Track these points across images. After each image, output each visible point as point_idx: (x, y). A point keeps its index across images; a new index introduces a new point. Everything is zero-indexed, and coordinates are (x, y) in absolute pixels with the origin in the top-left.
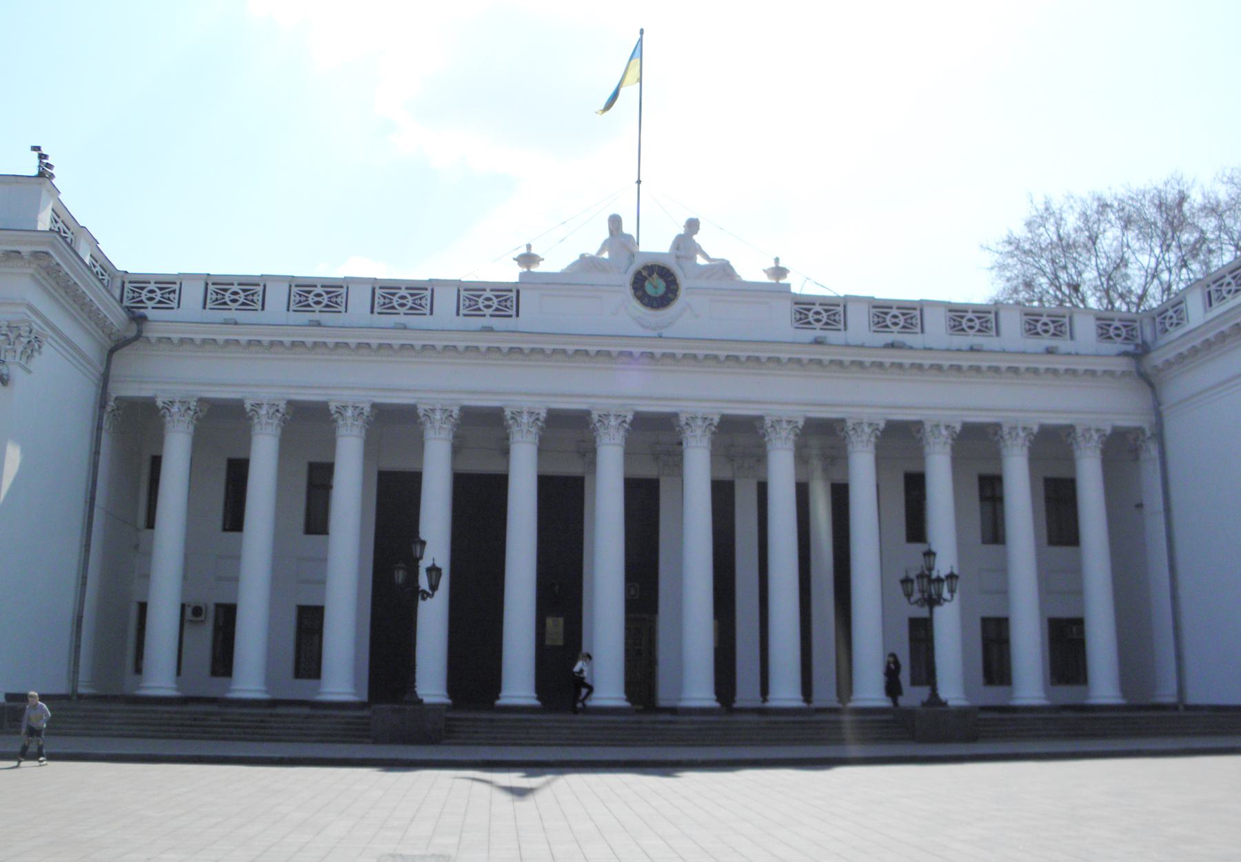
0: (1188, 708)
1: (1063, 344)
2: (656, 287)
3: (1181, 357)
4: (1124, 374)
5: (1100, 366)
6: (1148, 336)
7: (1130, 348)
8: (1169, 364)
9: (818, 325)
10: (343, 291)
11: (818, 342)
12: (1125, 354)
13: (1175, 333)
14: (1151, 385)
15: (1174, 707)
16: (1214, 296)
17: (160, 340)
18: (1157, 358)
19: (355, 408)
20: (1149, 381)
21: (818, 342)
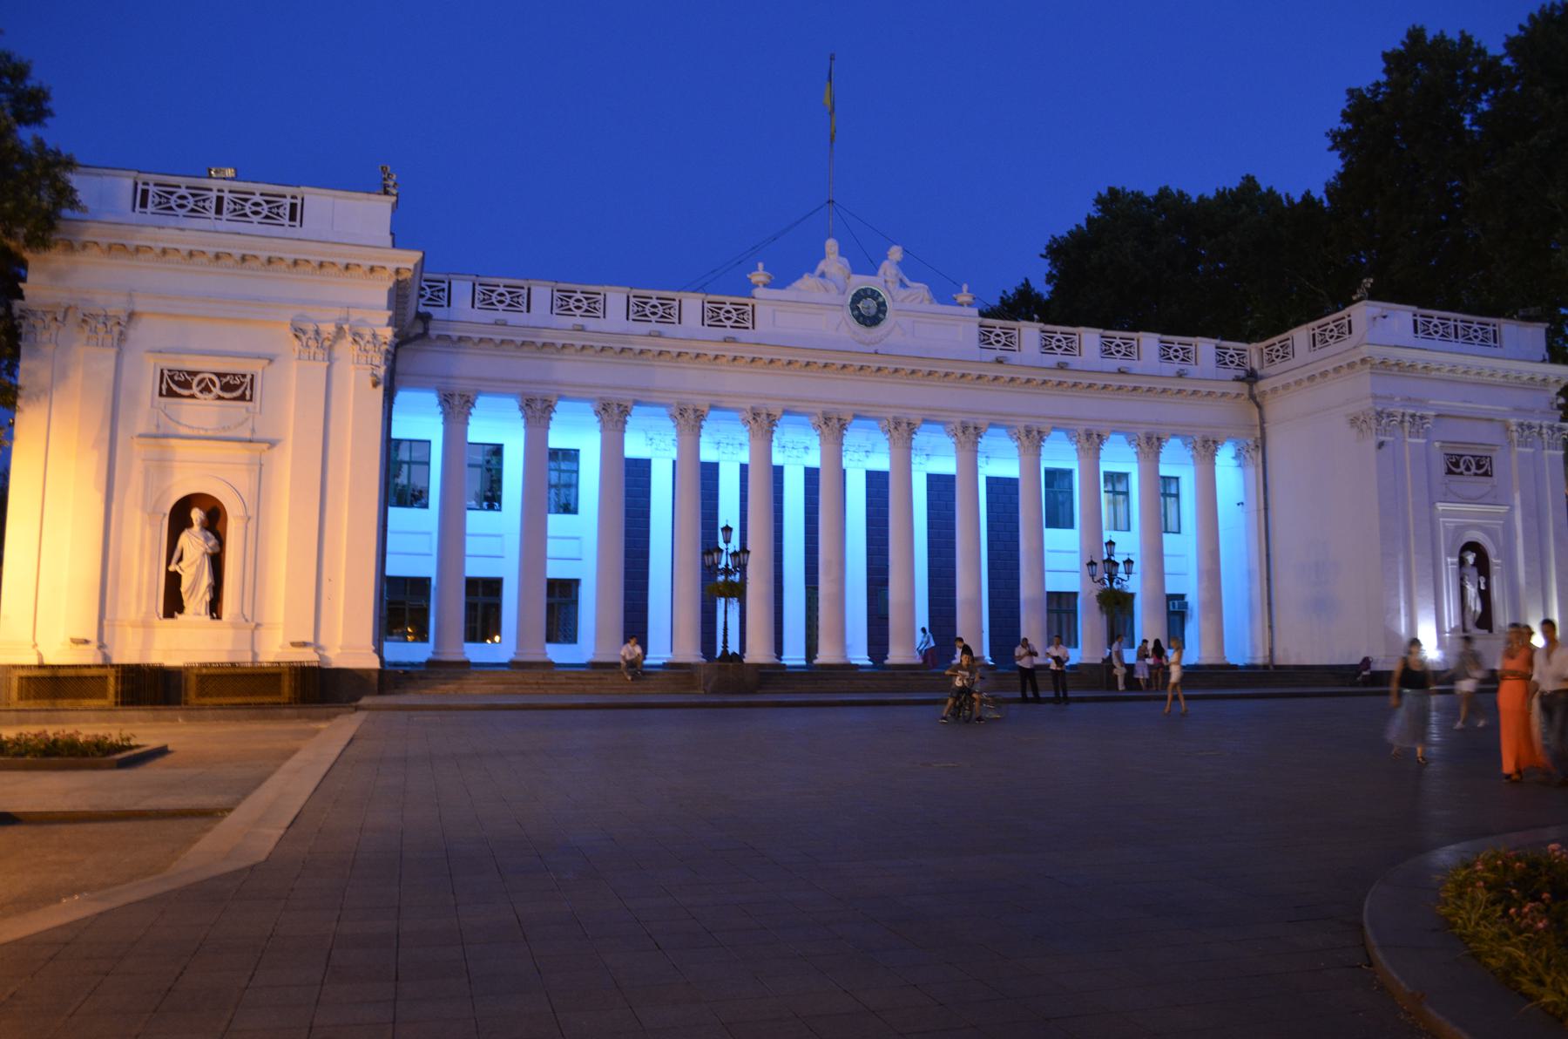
0: (1276, 667)
1: (1189, 368)
2: (868, 306)
3: (1286, 387)
4: (1238, 395)
5: (1218, 388)
6: (1256, 365)
7: (1242, 373)
8: (1275, 390)
9: (998, 346)
10: (601, 298)
11: (999, 361)
12: (1237, 379)
13: (1280, 366)
14: (1259, 406)
15: (1265, 667)
16: (1318, 338)
17: (439, 337)
18: (1263, 385)
19: (619, 405)
20: (1256, 401)
21: (999, 361)
